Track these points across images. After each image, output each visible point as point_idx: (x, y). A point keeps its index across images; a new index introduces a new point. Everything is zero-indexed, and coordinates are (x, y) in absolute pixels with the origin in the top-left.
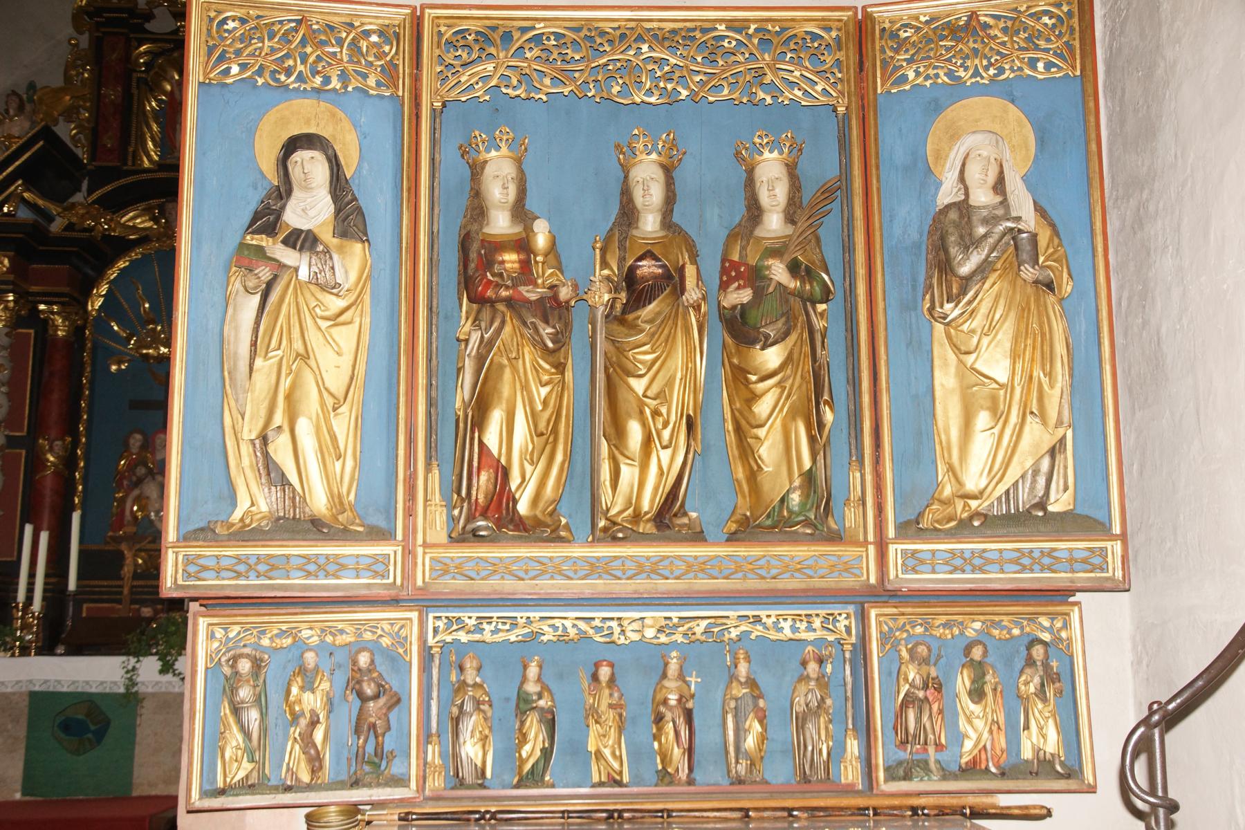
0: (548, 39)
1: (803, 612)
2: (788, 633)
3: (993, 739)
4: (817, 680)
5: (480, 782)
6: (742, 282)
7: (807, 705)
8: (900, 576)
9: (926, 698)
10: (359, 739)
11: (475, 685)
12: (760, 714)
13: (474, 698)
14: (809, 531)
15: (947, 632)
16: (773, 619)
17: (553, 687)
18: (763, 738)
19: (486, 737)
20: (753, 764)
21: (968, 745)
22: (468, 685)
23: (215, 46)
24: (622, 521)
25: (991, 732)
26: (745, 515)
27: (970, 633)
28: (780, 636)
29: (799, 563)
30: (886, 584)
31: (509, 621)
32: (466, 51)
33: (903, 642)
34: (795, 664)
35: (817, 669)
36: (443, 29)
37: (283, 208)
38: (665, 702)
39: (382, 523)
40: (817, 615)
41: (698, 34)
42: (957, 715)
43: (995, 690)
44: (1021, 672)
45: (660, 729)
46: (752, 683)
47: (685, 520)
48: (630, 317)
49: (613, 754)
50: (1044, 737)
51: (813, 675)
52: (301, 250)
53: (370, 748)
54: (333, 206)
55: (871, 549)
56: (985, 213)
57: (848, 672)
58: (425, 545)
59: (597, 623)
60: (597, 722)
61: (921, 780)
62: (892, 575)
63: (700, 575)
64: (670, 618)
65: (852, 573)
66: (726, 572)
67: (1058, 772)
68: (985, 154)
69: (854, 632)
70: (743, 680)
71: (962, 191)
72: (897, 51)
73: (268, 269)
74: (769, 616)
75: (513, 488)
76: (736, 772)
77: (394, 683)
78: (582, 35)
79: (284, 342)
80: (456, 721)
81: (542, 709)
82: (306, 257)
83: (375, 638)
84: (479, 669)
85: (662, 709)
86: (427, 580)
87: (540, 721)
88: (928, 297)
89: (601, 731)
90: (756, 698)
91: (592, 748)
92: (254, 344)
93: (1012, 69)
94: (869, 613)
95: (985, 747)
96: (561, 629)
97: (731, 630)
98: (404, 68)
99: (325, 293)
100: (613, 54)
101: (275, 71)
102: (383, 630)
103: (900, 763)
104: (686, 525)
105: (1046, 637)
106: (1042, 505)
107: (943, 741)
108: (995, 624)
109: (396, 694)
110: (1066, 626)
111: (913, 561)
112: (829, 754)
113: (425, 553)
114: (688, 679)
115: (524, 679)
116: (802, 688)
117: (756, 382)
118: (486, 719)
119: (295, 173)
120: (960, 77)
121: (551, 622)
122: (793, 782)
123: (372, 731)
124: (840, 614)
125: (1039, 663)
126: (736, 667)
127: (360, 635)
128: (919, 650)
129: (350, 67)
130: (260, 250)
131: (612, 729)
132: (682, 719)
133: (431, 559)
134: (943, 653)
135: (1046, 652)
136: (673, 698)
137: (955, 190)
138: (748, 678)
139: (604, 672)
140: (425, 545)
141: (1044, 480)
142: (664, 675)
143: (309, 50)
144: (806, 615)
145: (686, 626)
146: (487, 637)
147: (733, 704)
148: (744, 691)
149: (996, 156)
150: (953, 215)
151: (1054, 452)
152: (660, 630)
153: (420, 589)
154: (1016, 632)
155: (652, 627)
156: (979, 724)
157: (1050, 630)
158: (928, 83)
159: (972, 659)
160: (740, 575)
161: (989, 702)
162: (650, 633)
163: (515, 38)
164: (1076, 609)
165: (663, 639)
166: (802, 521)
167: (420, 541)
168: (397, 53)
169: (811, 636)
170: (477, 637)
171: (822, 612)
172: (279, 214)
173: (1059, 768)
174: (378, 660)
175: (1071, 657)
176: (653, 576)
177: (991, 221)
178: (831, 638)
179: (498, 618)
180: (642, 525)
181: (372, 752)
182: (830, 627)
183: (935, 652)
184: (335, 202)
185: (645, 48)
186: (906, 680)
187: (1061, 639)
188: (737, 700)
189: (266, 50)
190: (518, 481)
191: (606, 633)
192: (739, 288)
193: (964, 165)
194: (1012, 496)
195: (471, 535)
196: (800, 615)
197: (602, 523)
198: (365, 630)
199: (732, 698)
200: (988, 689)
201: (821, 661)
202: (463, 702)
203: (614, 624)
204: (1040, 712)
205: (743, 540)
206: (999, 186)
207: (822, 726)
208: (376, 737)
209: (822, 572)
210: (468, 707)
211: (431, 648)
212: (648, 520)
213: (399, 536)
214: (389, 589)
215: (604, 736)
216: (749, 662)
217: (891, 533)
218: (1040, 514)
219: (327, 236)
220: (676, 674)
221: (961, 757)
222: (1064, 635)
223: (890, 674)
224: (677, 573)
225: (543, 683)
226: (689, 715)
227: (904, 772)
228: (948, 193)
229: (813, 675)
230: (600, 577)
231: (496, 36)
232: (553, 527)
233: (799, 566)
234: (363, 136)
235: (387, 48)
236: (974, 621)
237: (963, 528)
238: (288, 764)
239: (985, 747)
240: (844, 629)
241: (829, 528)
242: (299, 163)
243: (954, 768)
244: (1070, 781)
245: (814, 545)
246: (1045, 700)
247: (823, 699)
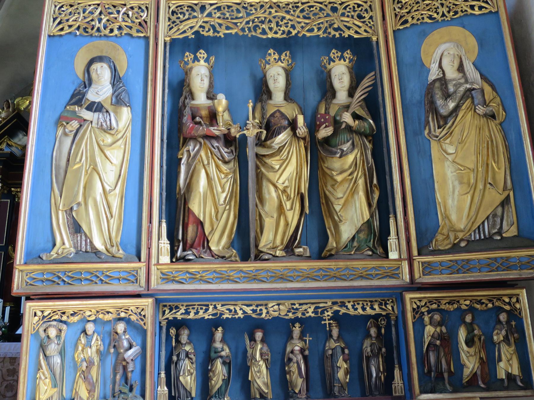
0: (224, 8)
2: (360, 311)
6: (327, 124)
16: (352, 303)
23: (56, 18)
32: (182, 15)
33: (426, 313)
36: (171, 5)
37: (87, 92)
41: (300, 5)
44: (494, 329)
48: (268, 142)
50: (511, 365)
52: (95, 111)
54: (112, 90)
56: (454, 82)
67: (519, 386)
68: (451, 53)
71: (441, 72)
72: (401, 8)
73: (77, 121)
75: (207, 233)
78: (241, 5)
79: (84, 158)
82: (96, 114)
88: (427, 128)
92: (68, 160)
93: (462, 11)
98: (151, 24)
99: (106, 134)
100: (257, 14)
101: (85, 29)
105: (507, 308)
106: (500, 233)
110: (518, 301)
111: (428, 268)
114: (305, 338)
117: (337, 175)
119: (94, 76)
120: (435, 18)
124: (389, 301)
127: (119, 314)
129: (123, 24)
130: (74, 112)
132: (302, 361)
137: (437, 72)
140: (158, 263)
141: (499, 220)
143: (103, 17)
149: (457, 53)
150: (437, 85)
151: (505, 203)
154: (490, 305)
157: (509, 304)
158: (419, 22)
163: (207, 8)
168: (147, 16)
169: (373, 313)
172: (84, 95)
173: (520, 384)
177: (457, 86)
178: (384, 313)
179: (198, 305)
182: (383, 307)
184: (113, 88)
185: (273, 11)
187: (516, 309)
189: (81, 17)
190: (210, 229)
192: (326, 127)
193: (441, 59)
194: (481, 230)
196: (366, 301)
198: (122, 312)
206: (461, 68)
217: (415, 252)
218: (499, 238)
219: (107, 106)
222: (518, 306)
228: (434, 74)
231: (197, 8)
234: (129, 57)
235: (142, 14)
237: (455, 248)
238: (76, 390)
240: (390, 308)
242: (95, 69)
246: (509, 344)
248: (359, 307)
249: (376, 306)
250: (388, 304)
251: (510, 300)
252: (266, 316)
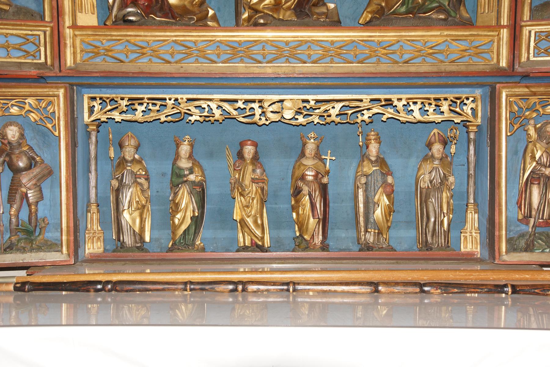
1: (432, 96)
2: (417, 115)
4: (441, 159)
5: (139, 245)
7: (431, 182)
8: (532, 58)
10: (11, 207)
11: (134, 161)
12: (388, 189)
13: (132, 172)
14: (442, 17)
17: (204, 163)
18: (390, 211)
19: (144, 207)
20: (380, 233)
22: (127, 161)
24: (264, 8)
26: (380, 5)
28: (410, 118)
29: (431, 48)
30: (516, 67)
31: (159, 103)
34: (421, 146)
35: (442, 150)
38: (303, 178)
39: (33, 6)
40: (446, 99)
45: (298, 201)
46: (381, 162)
47: (324, 10)
49: (255, 222)
51: (437, 155)
53: (24, 215)
55: (505, 33)
57: (472, 152)
58: (74, 26)
59: (240, 104)
60: (241, 195)
61: (543, 251)
62: (524, 59)
63: (336, 59)
64: (307, 101)
65: (483, 58)
66: (361, 57)
69: (480, 114)
70: (373, 159)
74: (399, 100)
76: (365, 239)
77: (45, 155)
80: (118, 191)
81: (193, 182)
83: (23, 113)
84: (137, 148)
85: (300, 184)
86: (78, 61)
87: (191, 193)
89: (245, 203)
90: (384, 175)
91: (237, 216)
94: (500, 93)
96: (207, 110)
97: (364, 112)
102: (30, 105)
103: (522, 235)
104: (323, 13)
109: (47, 167)
112: (449, 225)
113: (75, 36)
114: (323, 157)
115: (177, 157)
116: (428, 167)
118: (143, 191)
121: (197, 103)
122: (415, 248)
123: (25, 201)
126: (367, 147)
131: (255, 201)
132: (317, 193)
133: (82, 41)
136: (310, 175)
138: (378, 157)
139: (249, 150)
142: (303, 154)
144: (436, 99)
145: (323, 108)
146: (139, 116)
147: (363, 180)
148: (374, 168)
152: (298, 112)
153: (70, 69)
155: (290, 109)
160: (374, 59)
162: (288, 115)
165: (301, 119)
166: (436, 7)
167: (68, 22)
169: (438, 118)
170: (129, 117)
171: (451, 97)
174: (29, 134)
176: (291, 60)
179: (149, 99)
180: (282, 12)
181: (26, 219)
182: (458, 110)
186: (533, 157)
188: (367, 176)
191: (248, 114)
195: (122, 22)
197: (246, 15)
198: (12, 105)
199: (362, 175)
201: (445, 143)
202: (123, 175)
203: (256, 106)
205: (379, 25)
207: (445, 200)
208: (29, 205)
209: (453, 57)
210: (127, 180)
211: (87, 125)
212: (289, 8)
213: (47, 19)
214: (39, 69)
215: (248, 207)
216: (380, 143)
217: (526, 15)
220: (313, 153)
223: (516, 153)
224: (314, 58)
225: (195, 160)
226: (324, 189)
227: (526, 244)
229: (437, 155)
230: (242, 61)
232: (200, 15)
233: (431, 51)
240: (470, 112)
241: (461, 16)
245: (447, 30)
247: (445, 177)
248: (415, 108)
249: (445, 107)
250: (466, 104)
252: (260, 119)
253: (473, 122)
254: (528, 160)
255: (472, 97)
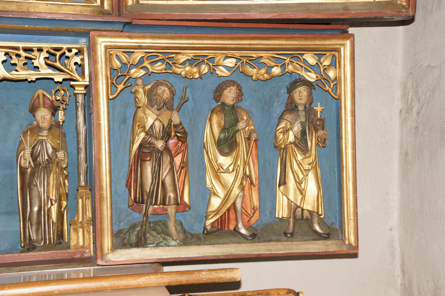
1: (21, 45)
3: (244, 196)
9: (167, 149)
15: (195, 70)
21: (216, 202)
25: (242, 187)
27: (222, 72)
33: (140, 82)
34: (24, 111)
42: (205, 168)
43: (249, 139)
44: (281, 118)
50: (302, 192)
51: (45, 125)
67: (316, 232)
95: (234, 204)
105: (311, 77)
107: (186, 199)
108: (252, 61)
110: (335, 63)
124: (70, 50)
125: (301, 108)
128: (159, 92)
134: (189, 95)
135: (310, 95)
144: (26, 50)
156: (229, 178)
157: (315, 68)
159: (223, 104)
161: (241, 153)
164: (348, 43)
169: (32, 75)
171: (46, 46)
173: (317, 228)
175: (338, 100)
182: (58, 64)
183: (179, 94)
187: (327, 79)
196: (17, 49)
200: (241, 138)
204: (299, 164)
221: (206, 218)
222: (331, 74)
223: (124, 121)
227: (137, 237)
236: (227, 57)
239: (234, 204)
243: (198, 229)
244: (329, 242)
246: (305, 150)
251: (319, 60)
253: (79, 81)
254: (137, 130)
255: (76, 48)
